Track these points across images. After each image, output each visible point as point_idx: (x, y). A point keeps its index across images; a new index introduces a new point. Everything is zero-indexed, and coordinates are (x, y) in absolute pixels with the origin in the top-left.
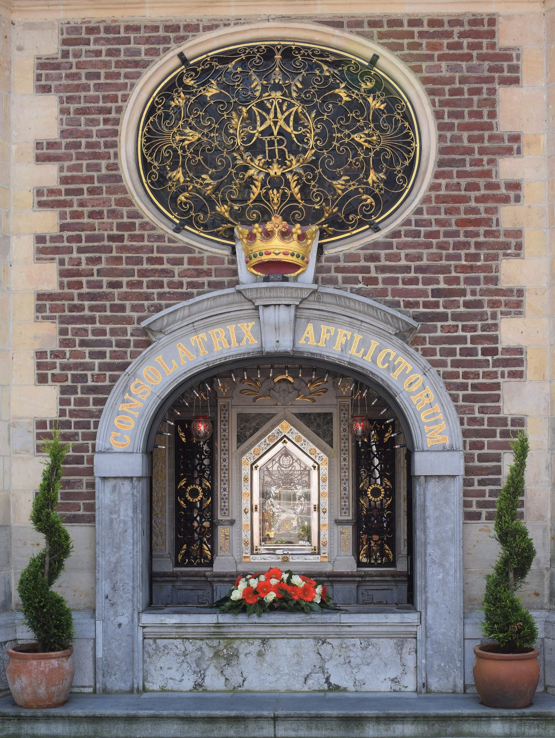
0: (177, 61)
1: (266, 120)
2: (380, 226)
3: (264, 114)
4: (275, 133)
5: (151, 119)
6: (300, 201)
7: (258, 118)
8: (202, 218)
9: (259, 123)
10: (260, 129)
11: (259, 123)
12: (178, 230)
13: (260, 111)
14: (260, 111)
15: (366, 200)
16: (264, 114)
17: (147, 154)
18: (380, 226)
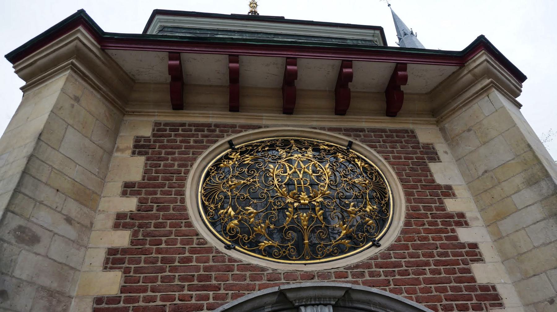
0: (227, 146)
1: (292, 168)
2: (380, 242)
3: (291, 166)
4: (301, 176)
5: (208, 179)
6: (322, 222)
7: (288, 168)
8: (246, 239)
9: (288, 170)
10: (289, 172)
11: (288, 170)
12: (228, 247)
13: (289, 164)
14: (289, 164)
15: (368, 221)
16: (291, 166)
17: (205, 200)
18: (380, 242)
